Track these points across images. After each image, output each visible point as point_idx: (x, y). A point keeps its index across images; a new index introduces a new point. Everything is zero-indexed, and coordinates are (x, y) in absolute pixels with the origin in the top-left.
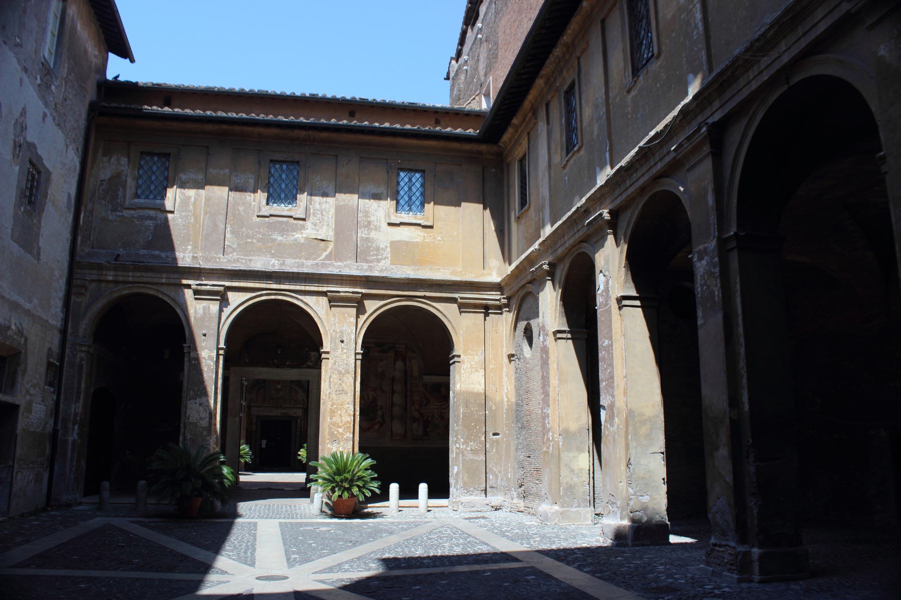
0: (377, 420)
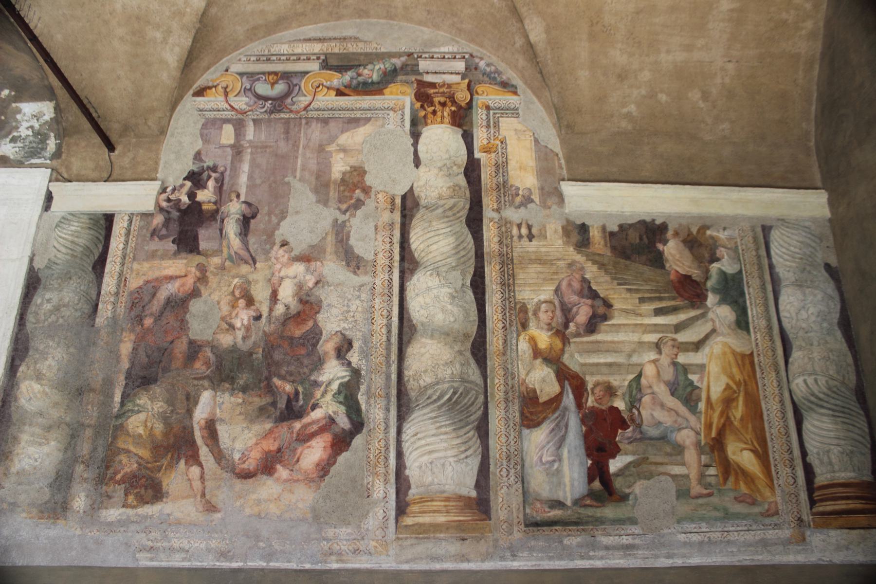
0: (317, 414)
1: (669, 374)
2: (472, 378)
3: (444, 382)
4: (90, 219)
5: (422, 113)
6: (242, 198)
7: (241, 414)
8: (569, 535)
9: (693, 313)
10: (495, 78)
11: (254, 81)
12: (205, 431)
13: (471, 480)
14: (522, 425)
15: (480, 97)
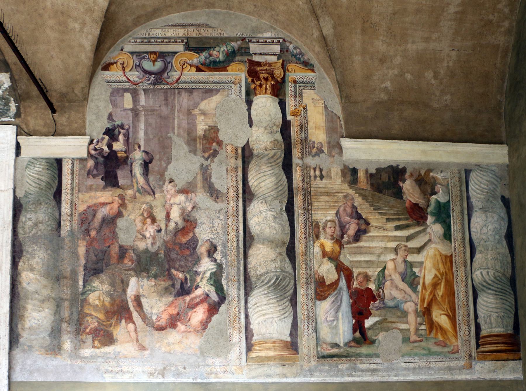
0: (199, 292)
1: (401, 267)
2: (287, 270)
3: (271, 272)
4: (47, 162)
5: (253, 86)
7: (154, 292)
8: (341, 363)
9: (418, 229)
10: (299, 59)
12: (134, 302)
13: (287, 332)
14: (316, 298)
15: (290, 74)
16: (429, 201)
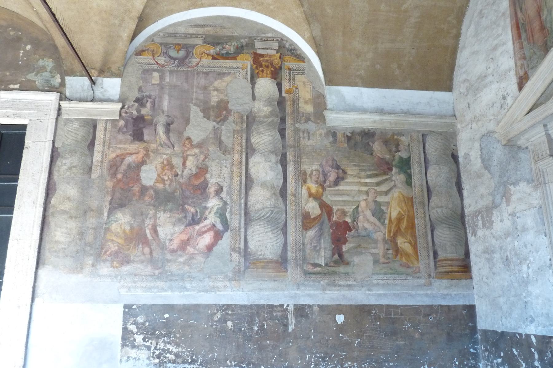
0: (207, 222)
1: (373, 206)
2: (280, 206)
4: (84, 121)
5: (257, 71)
6: (166, 113)
7: (169, 222)
10: (293, 53)
11: (168, 48)
14: (303, 228)
16: (394, 157)
